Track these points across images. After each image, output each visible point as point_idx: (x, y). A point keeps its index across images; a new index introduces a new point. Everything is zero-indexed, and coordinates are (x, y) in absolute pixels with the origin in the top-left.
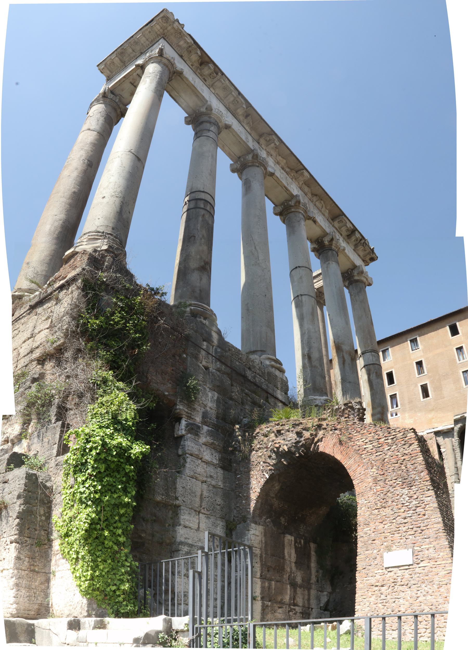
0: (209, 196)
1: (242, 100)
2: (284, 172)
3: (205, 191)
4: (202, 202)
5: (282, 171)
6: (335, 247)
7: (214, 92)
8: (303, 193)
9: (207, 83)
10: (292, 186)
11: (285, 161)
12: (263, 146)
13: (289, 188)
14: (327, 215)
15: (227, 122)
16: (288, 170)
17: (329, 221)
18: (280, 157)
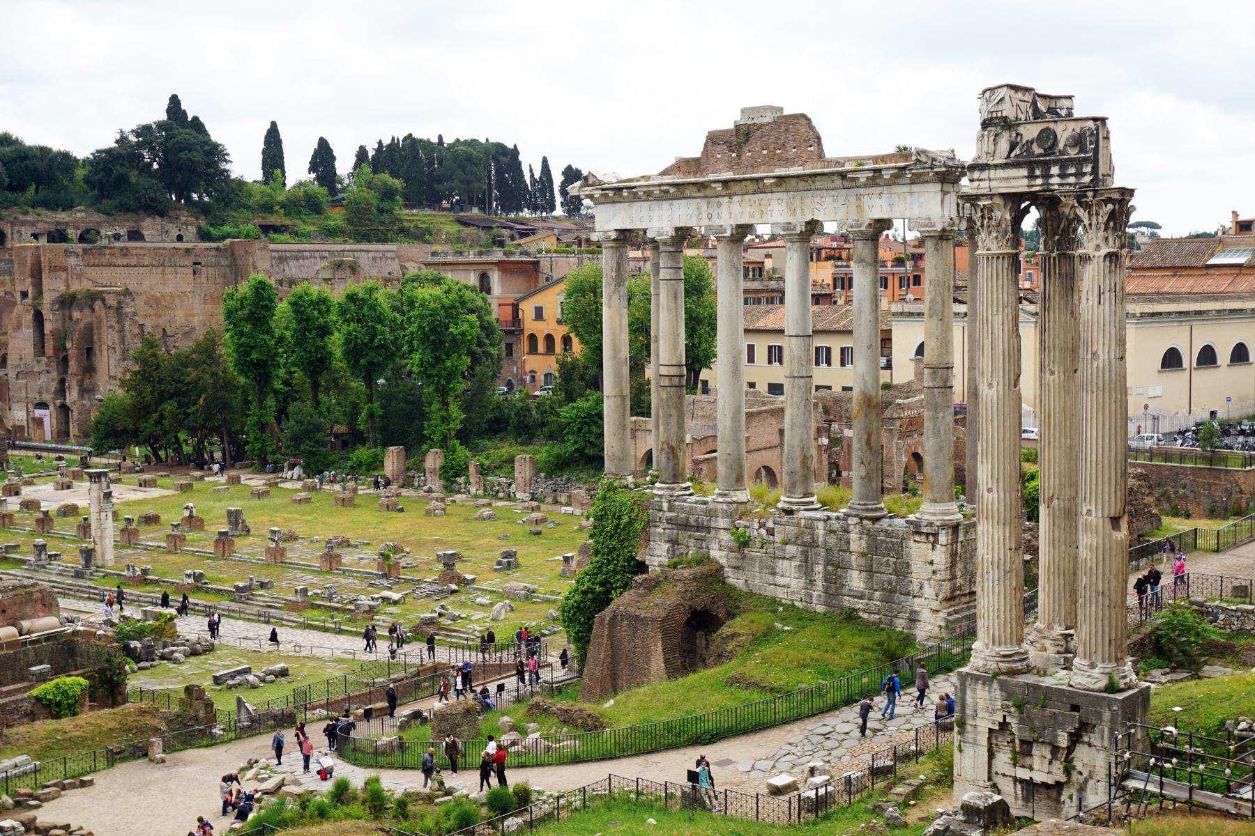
2: (757, 196)
13: (764, 220)
14: (838, 182)
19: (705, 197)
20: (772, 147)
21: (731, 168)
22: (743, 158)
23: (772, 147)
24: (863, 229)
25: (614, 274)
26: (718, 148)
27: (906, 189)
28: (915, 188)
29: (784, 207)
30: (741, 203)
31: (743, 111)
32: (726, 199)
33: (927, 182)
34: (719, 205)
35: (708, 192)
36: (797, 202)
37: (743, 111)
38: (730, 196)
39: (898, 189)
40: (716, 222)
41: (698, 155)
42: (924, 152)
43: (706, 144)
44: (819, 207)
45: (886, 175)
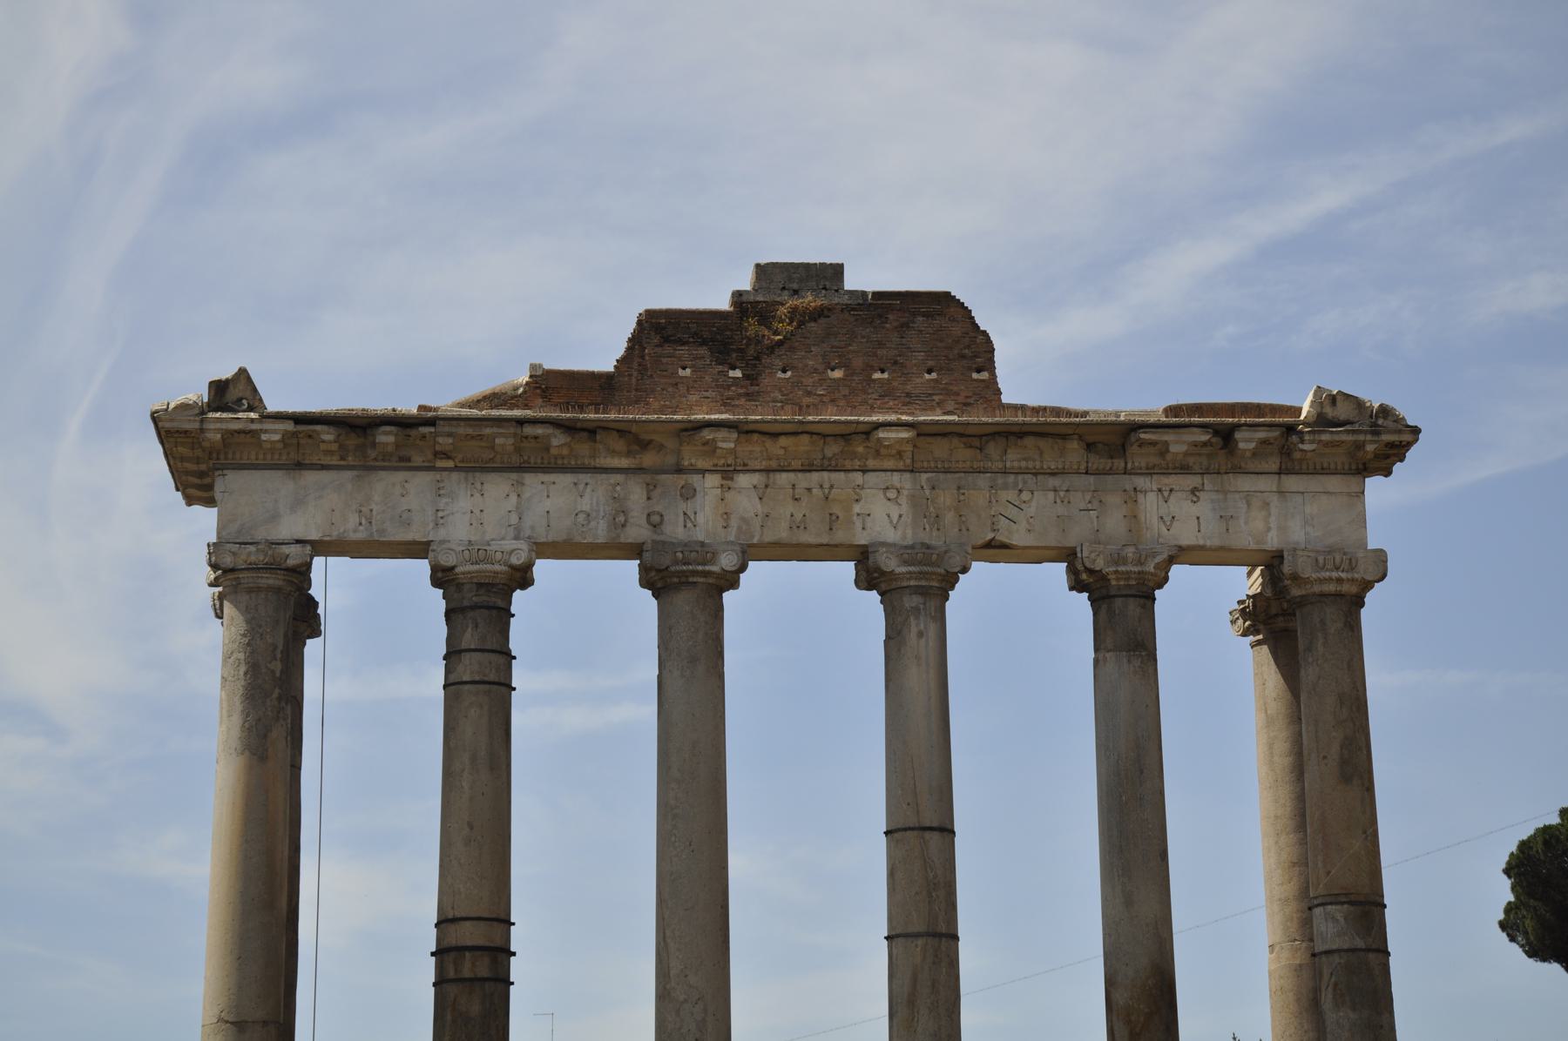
0: (468, 924)
1: (540, 430)
2: (815, 476)
3: (458, 915)
4: (453, 955)
5: (803, 480)
6: (1118, 579)
7: (450, 464)
8: (924, 476)
9: (418, 460)
10: (857, 508)
11: (805, 438)
12: (701, 464)
13: (840, 536)
15: (515, 561)
16: (832, 449)
17: (1097, 473)
18: (783, 441)
19: (639, 470)
20: (858, 362)
21: (726, 405)
22: (766, 381)
23: (858, 362)
24: (1150, 567)
25: (277, 666)
26: (683, 351)
27: (1266, 483)
28: (1292, 482)
29: (905, 508)
30: (762, 493)
31: (762, 271)
32: (712, 480)
33: (1324, 471)
34: (688, 493)
35: (649, 459)
36: (946, 498)
37: (762, 271)
38: (728, 473)
39: (1245, 483)
40: (675, 530)
41: (608, 365)
42: (1348, 396)
43: (635, 342)
44: (1012, 512)
45: (1246, 441)
